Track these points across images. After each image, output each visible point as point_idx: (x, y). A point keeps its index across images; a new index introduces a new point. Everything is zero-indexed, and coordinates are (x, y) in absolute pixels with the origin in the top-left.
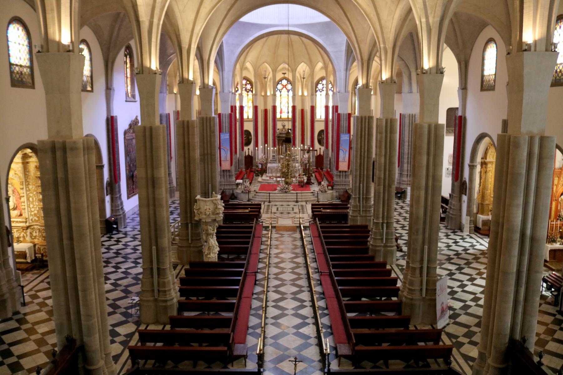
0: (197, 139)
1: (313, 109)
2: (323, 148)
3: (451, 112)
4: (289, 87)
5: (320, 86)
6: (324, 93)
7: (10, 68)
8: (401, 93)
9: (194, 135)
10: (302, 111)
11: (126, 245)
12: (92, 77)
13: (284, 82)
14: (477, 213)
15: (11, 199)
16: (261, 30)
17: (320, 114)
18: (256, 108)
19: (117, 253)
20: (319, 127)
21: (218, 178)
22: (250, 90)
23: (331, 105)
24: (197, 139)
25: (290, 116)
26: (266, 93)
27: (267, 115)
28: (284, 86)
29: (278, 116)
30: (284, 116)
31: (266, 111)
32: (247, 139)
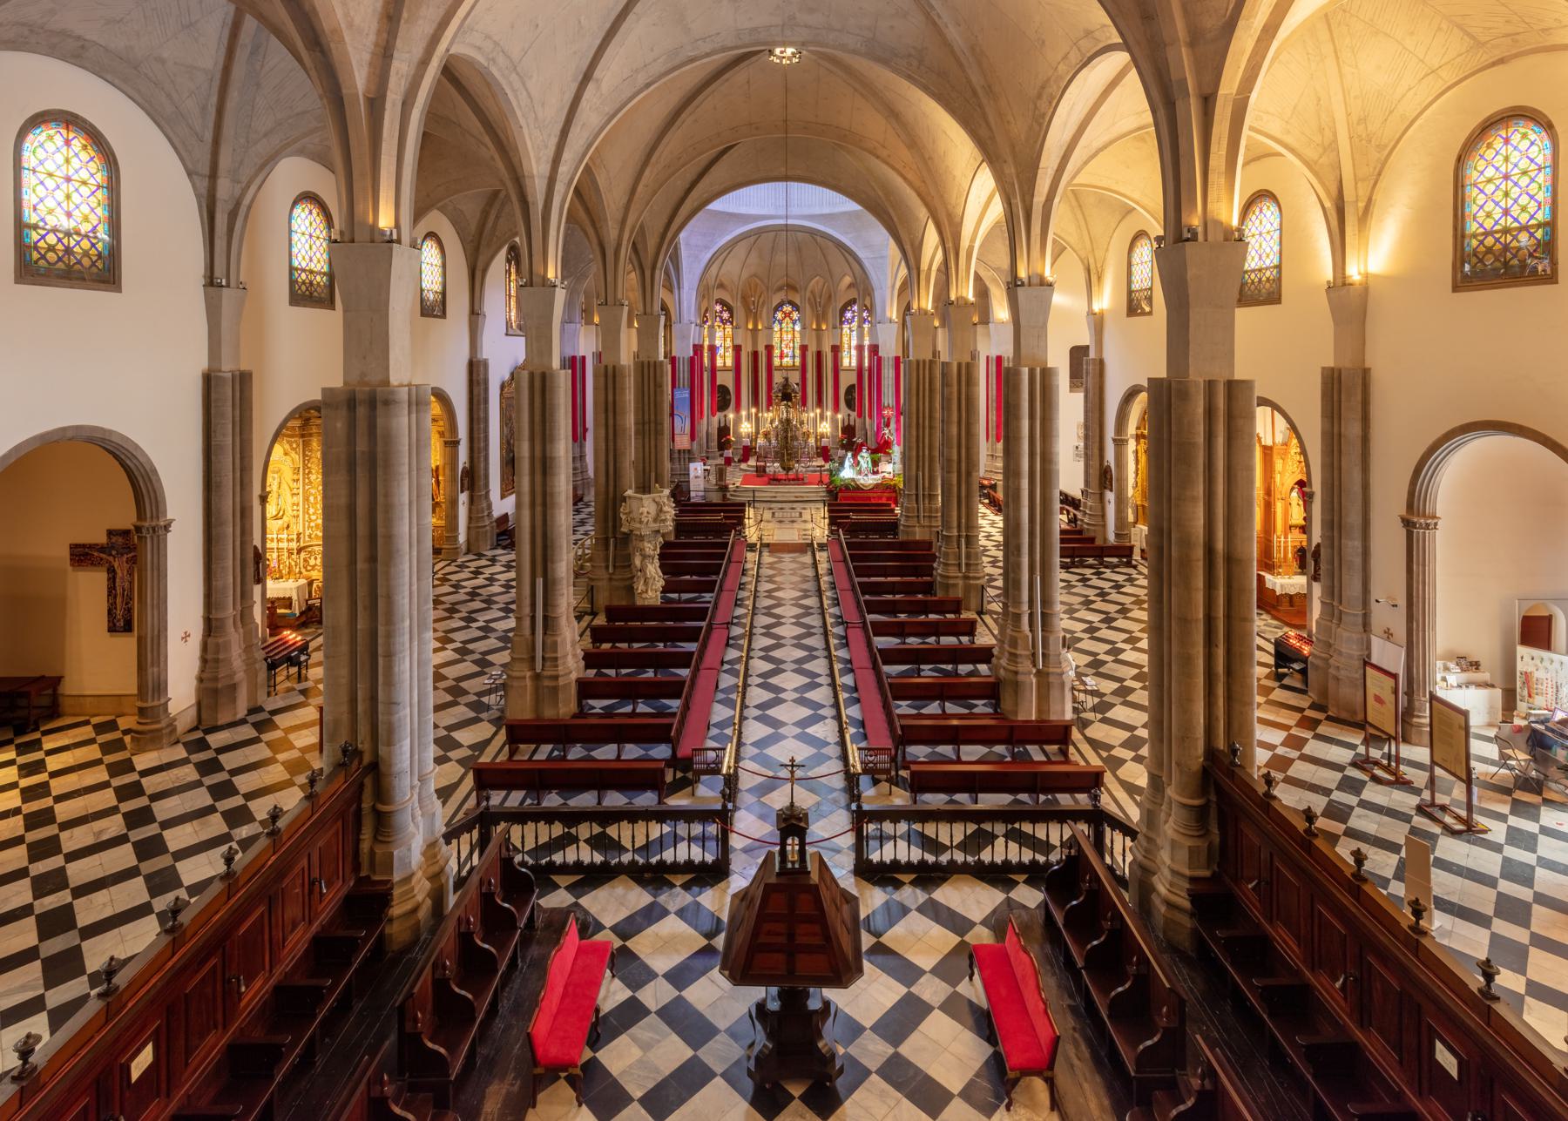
0: (629, 397)
1: (836, 350)
2: (854, 414)
3: (1078, 353)
4: (795, 315)
5: (849, 315)
6: (855, 325)
7: (291, 274)
8: (987, 323)
9: (623, 389)
11: (491, 580)
12: (444, 293)
13: (787, 308)
14: (1136, 522)
15: (272, 499)
16: (746, 223)
17: (849, 360)
18: (737, 349)
19: (473, 594)
20: (847, 380)
21: (667, 465)
23: (867, 342)
24: (629, 397)
25: (798, 361)
26: (755, 325)
27: (758, 362)
28: (787, 315)
29: (776, 362)
30: (787, 361)
31: (755, 354)
32: (723, 399)
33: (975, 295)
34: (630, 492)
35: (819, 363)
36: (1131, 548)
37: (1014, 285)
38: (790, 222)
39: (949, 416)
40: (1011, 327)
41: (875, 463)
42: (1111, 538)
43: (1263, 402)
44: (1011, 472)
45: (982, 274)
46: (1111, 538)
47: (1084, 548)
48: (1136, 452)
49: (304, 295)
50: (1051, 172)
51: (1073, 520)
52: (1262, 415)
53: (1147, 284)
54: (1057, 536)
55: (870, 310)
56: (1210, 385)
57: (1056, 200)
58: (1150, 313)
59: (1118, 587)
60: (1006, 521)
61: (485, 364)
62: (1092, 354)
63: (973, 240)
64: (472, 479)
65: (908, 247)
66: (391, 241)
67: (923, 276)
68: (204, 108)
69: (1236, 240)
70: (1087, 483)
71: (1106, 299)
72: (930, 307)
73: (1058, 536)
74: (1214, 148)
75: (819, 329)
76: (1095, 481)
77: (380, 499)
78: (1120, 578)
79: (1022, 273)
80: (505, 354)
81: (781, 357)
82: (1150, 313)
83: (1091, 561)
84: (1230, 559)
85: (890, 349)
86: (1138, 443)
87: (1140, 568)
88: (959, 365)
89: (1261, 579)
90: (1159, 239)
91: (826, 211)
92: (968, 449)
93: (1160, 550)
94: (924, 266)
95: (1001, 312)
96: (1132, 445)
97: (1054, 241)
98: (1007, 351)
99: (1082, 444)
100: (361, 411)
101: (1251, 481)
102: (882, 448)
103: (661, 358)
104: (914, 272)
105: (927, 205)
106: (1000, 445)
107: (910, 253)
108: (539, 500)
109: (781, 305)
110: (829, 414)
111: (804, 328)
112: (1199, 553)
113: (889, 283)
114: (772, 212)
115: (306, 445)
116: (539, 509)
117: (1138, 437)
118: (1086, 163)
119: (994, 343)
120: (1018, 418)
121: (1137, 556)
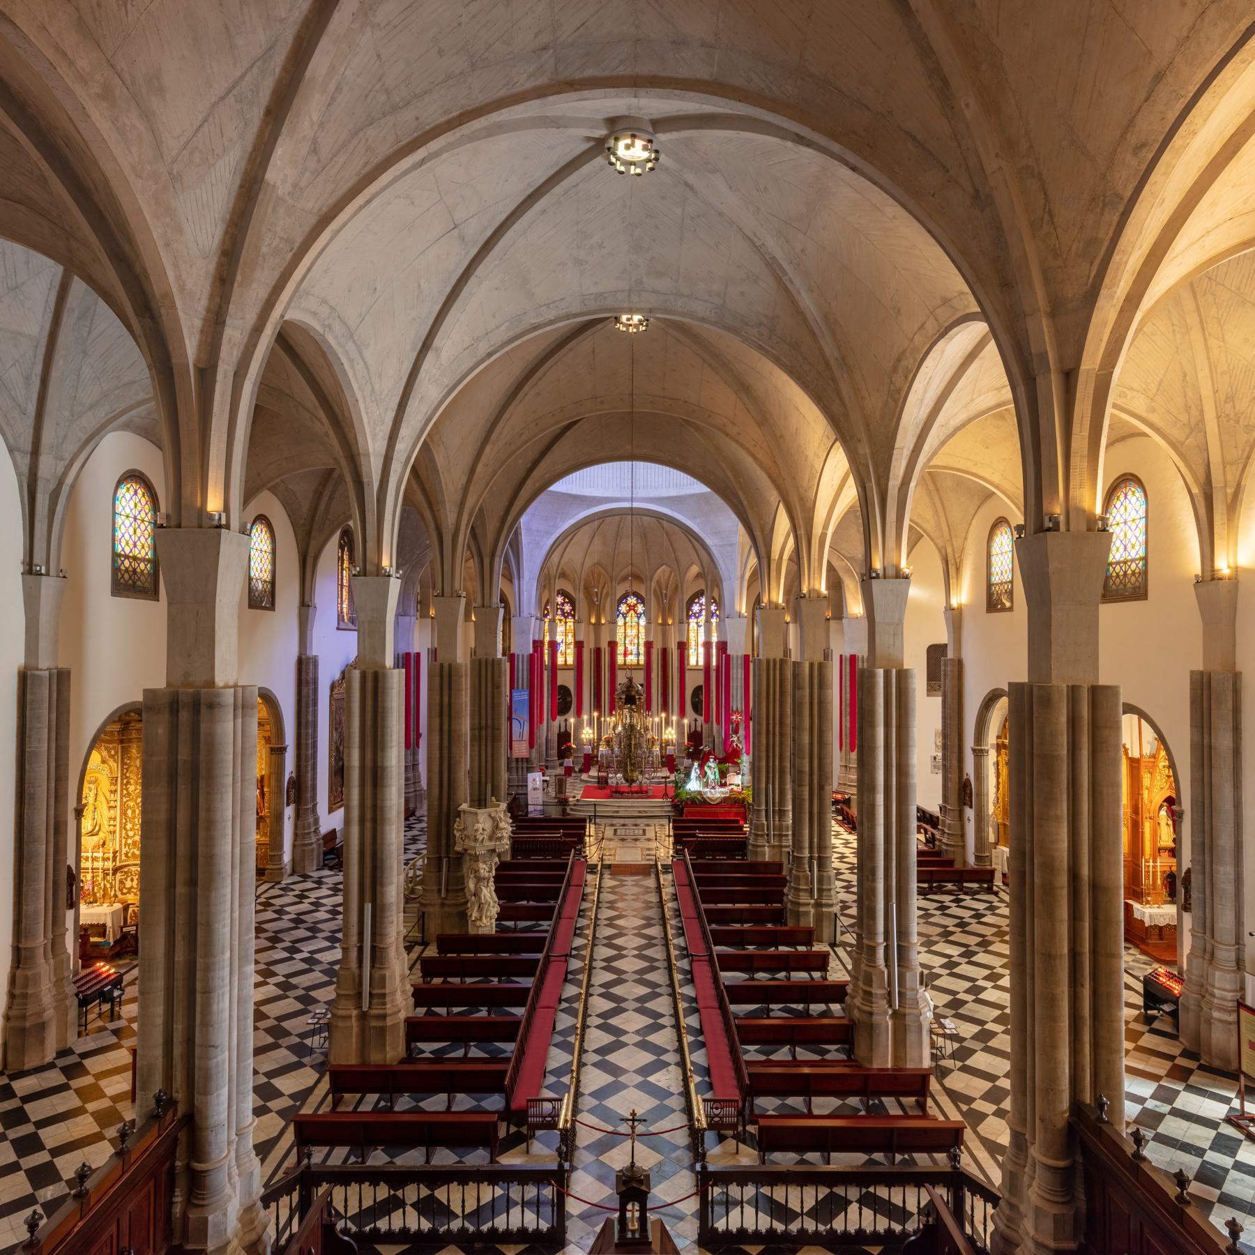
0: (465, 699)
1: (683, 647)
2: (701, 719)
3: (935, 653)
4: (640, 608)
5: (696, 608)
6: (702, 619)
7: (114, 561)
10: (665, 652)
11: (317, 905)
12: (273, 583)
13: (632, 600)
14: (997, 843)
15: (88, 813)
16: (589, 506)
17: (696, 658)
18: (579, 646)
19: (298, 921)
21: (504, 775)
22: (569, 614)
23: (714, 639)
24: (465, 699)
25: (642, 659)
26: (598, 619)
27: (598, 657)
28: (632, 608)
29: (620, 660)
30: (631, 659)
31: (598, 651)
32: (564, 702)
33: (828, 588)
34: (464, 806)
35: (665, 658)
36: (992, 872)
37: (868, 577)
38: (636, 505)
39: (801, 721)
40: (865, 624)
41: (723, 774)
42: (971, 860)
43: (1129, 709)
44: (866, 785)
45: (836, 564)
46: (971, 860)
47: (943, 872)
48: (997, 763)
49: (129, 583)
50: (906, 453)
51: (931, 840)
52: (1129, 723)
53: (1007, 577)
54: (913, 858)
55: (719, 604)
56: (1074, 691)
57: (913, 484)
58: (1011, 609)
59: (978, 916)
60: (860, 840)
61: (315, 661)
62: (950, 654)
63: (826, 527)
64: (300, 791)
65: (758, 534)
66: (219, 527)
67: (773, 566)
68: (28, 378)
69: (1098, 530)
70: (945, 798)
71: (963, 596)
72: (780, 601)
73: (915, 859)
74: (1076, 428)
75: (665, 624)
76: (953, 797)
77: (202, 815)
78: (981, 906)
79: (877, 565)
80: (335, 650)
81: (625, 655)
82: (1011, 609)
83: (950, 886)
84: (1096, 887)
85: (738, 649)
86: (999, 754)
87: (1002, 894)
88: (811, 665)
89: (1128, 908)
90: (1019, 529)
91: (673, 493)
92: (820, 759)
93: (1022, 875)
94: (775, 554)
95: (855, 607)
96: (992, 757)
97: (911, 528)
98: (861, 650)
99: (940, 754)
100: (184, 715)
101: (1117, 800)
102: (729, 758)
103: (499, 655)
104: (765, 561)
105: (778, 488)
106: (854, 755)
107: (760, 539)
108: (369, 815)
109: (625, 596)
110: (674, 718)
111: (649, 622)
112: (1063, 880)
113: (739, 574)
114: (617, 494)
115: (125, 751)
116: (368, 825)
117: (999, 747)
118: (943, 443)
119: (847, 642)
120: (872, 725)
121: (998, 881)
